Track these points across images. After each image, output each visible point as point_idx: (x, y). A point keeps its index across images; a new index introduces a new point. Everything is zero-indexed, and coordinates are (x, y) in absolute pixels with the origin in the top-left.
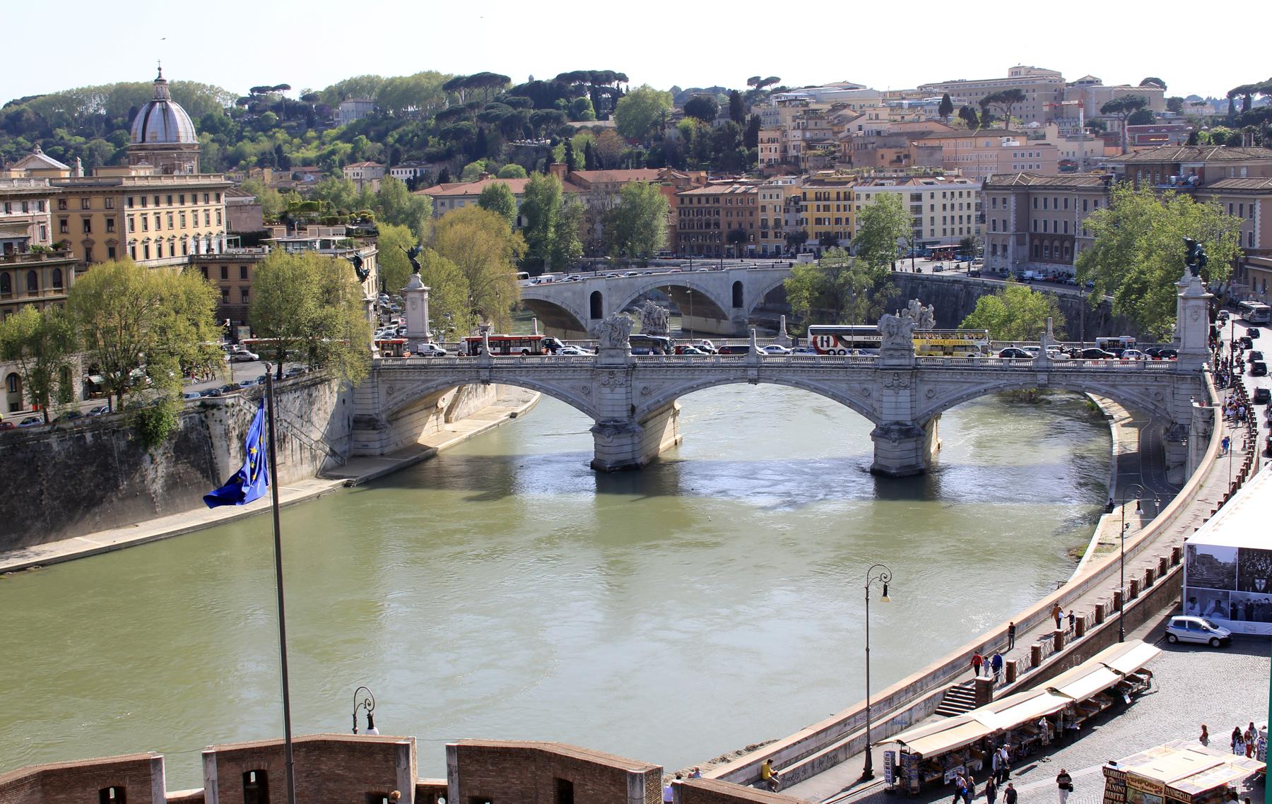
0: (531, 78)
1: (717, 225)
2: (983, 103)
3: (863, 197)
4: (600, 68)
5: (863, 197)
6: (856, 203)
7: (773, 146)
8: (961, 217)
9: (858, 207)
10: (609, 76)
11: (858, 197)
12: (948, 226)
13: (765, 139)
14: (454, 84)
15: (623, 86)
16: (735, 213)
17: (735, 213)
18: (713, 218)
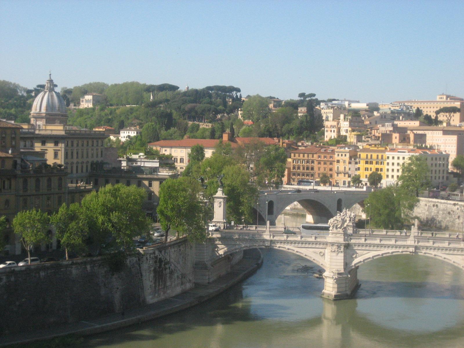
0: (188, 88)
1: (312, 169)
2: (437, 113)
3: (391, 158)
4: (227, 84)
5: (391, 158)
6: (388, 161)
7: (333, 130)
8: (439, 171)
9: (388, 164)
10: (232, 89)
11: (388, 158)
12: (437, 175)
13: (329, 126)
14: (150, 89)
15: (238, 94)
16: (322, 163)
17: (322, 163)
18: (310, 165)
